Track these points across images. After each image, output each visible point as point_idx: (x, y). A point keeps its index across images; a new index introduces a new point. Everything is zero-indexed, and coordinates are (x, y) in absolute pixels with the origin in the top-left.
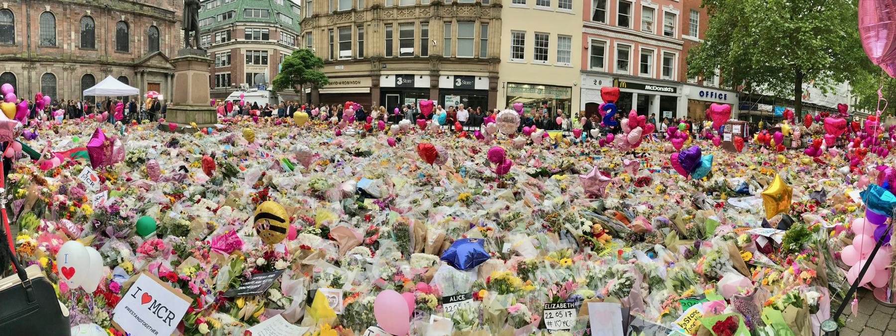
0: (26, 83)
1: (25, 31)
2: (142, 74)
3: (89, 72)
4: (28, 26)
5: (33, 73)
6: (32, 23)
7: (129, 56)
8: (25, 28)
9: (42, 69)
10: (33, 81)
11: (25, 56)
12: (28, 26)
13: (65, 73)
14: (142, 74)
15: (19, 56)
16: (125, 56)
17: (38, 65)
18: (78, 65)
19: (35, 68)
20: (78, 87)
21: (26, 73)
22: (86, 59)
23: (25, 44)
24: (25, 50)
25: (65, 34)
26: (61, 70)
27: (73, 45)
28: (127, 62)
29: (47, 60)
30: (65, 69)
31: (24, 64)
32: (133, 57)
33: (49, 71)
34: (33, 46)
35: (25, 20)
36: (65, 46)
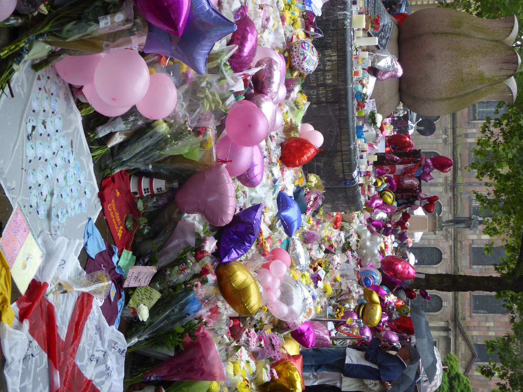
2: (446, 329)
3: (444, 256)
5: (440, 189)
7: (467, 314)
11: (460, 180)
14: (446, 329)
15: (459, 172)
16: (467, 307)
17: (450, 194)
18: (451, 243)
19: (446, 191)
22: (459, 254)
24: (466, 180)
28: (460, 311)
29: (455, 206)
31: (450, 179)
32: (468, 319)
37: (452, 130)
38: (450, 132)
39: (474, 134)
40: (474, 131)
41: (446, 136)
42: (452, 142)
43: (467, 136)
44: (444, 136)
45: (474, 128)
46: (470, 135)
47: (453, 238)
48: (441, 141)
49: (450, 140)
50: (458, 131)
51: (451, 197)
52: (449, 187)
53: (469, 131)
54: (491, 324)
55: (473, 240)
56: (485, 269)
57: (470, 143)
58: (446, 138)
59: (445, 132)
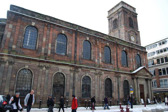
0: (72, 81)
1: (73, 49)
4: (76, 45)
6: (78, 44)
8: (73, 47)
9: (83, 73)
10: (76, 80)
12: (76, 45)
13: (96, 77)
17: (80, 70)
19: (78, 72)
20: (103, 86)
21: (72, 74)
23: (73, 55)
25: (96, 54)
26: (94, 75)
27: (100, 60)
30: (96, 74)
33: (87, 75)
34: (78, 58)
35: (74, 42)
36: (96, 61)
37: (41, 63)
38: (42, 64)
39: (45, 49)
40: (43, 49)
41: (44, 67)
42: (49, 64)
43: (46, 54)
44: (44, 69)
45: (41, 48)
46: (46, 52)
47: (101, 71)
48: (47, 71)
49: (48, 65)
51: (82, 70)
52: (76, 70)
53: (43, 52)
54: (131, 59)
55: (102, 61)
56: (113, 58)
57: (51, 53)
58: (46, 67)
59: (41, 67)
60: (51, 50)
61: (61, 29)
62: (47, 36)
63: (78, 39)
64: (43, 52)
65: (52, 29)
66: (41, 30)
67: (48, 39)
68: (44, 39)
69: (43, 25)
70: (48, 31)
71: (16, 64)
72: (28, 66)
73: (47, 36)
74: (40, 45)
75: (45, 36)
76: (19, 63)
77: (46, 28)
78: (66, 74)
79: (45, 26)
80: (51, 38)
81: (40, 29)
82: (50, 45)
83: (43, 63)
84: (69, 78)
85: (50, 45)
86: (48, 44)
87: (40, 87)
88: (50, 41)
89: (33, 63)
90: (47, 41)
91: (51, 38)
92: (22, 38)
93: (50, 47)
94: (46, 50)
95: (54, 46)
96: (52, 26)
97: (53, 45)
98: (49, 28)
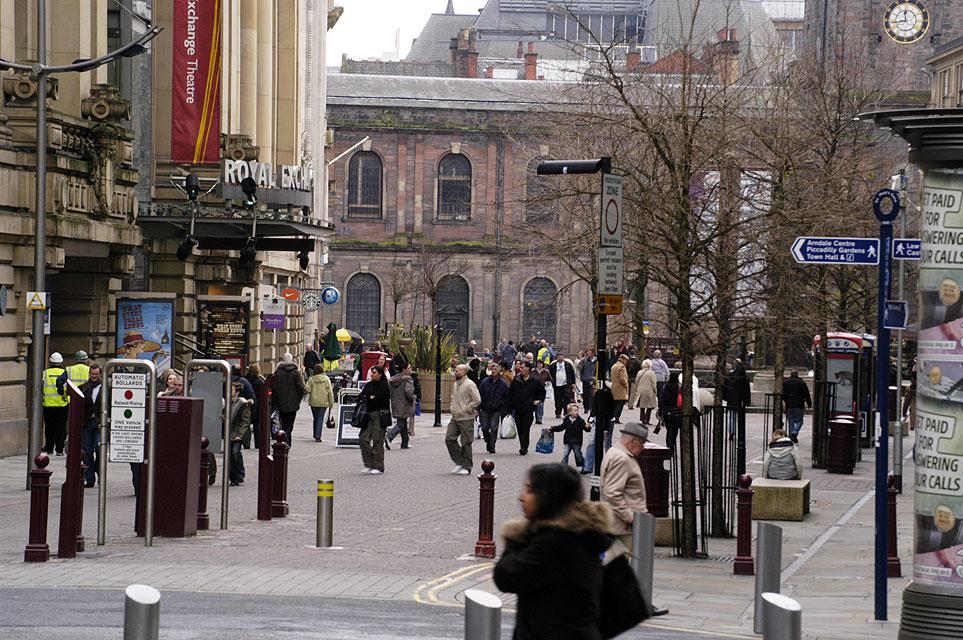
0: (490, 297)
17: (515, 261)
21: (489, 276)
31: (487, 260)
33: (541, 274)
35: (492, 175)
39: (406, 213)
40: (401, 213)
43: (410, 227)
44: (409, 267)
50: (403, 242)
51: (521, 262)
52: (502, 264)
53: (401, 222)
57: (424, 221)
58: (412, 266)
60: (424, 212)
61: (449, 138)
62: (407, 173)
63: (508, 161)
64: (401, 222)
65: (420, 147)
66: (388, 158)
67: (411, 182)
68: (402, 185)
69: (393, 142)
70: (409, 158)
71: (338, 263)
72: (366, 268)
73: (410, 173)
74: (391, 203)
75: (401, 174)
76: (347, 260)
77: (402, 149)
78: (471, 279)
79: (399, 142)
80: (419, 177)
81: (388, 157)
82: (418, 198)
83: (405, 254)
84: (481, 288)
85: (418, 198)
86: (414, 198)
87: (403, 318)
88: (419, 188)
89: (377, 257)
90: (410, 187)
91: (419, 177)
92: (344, 195)
93: (419, 205)
94: (410, 215)
95: (432, 199)
96: (420, 137)
97: (427, 199)
98: (412, 145)
